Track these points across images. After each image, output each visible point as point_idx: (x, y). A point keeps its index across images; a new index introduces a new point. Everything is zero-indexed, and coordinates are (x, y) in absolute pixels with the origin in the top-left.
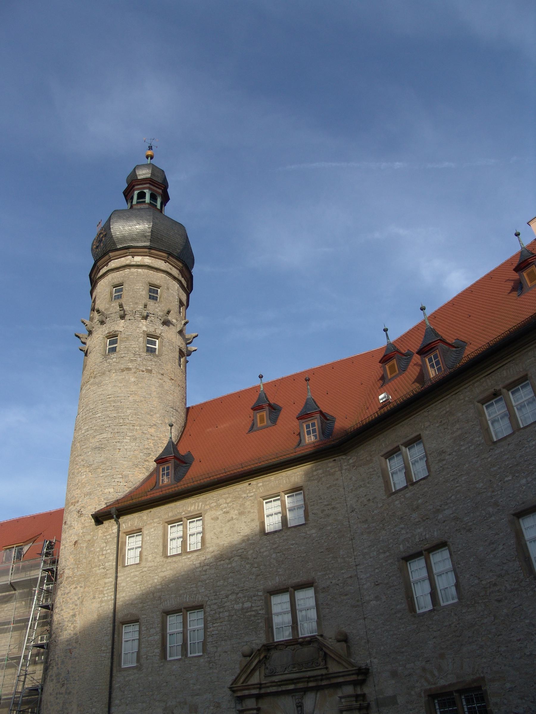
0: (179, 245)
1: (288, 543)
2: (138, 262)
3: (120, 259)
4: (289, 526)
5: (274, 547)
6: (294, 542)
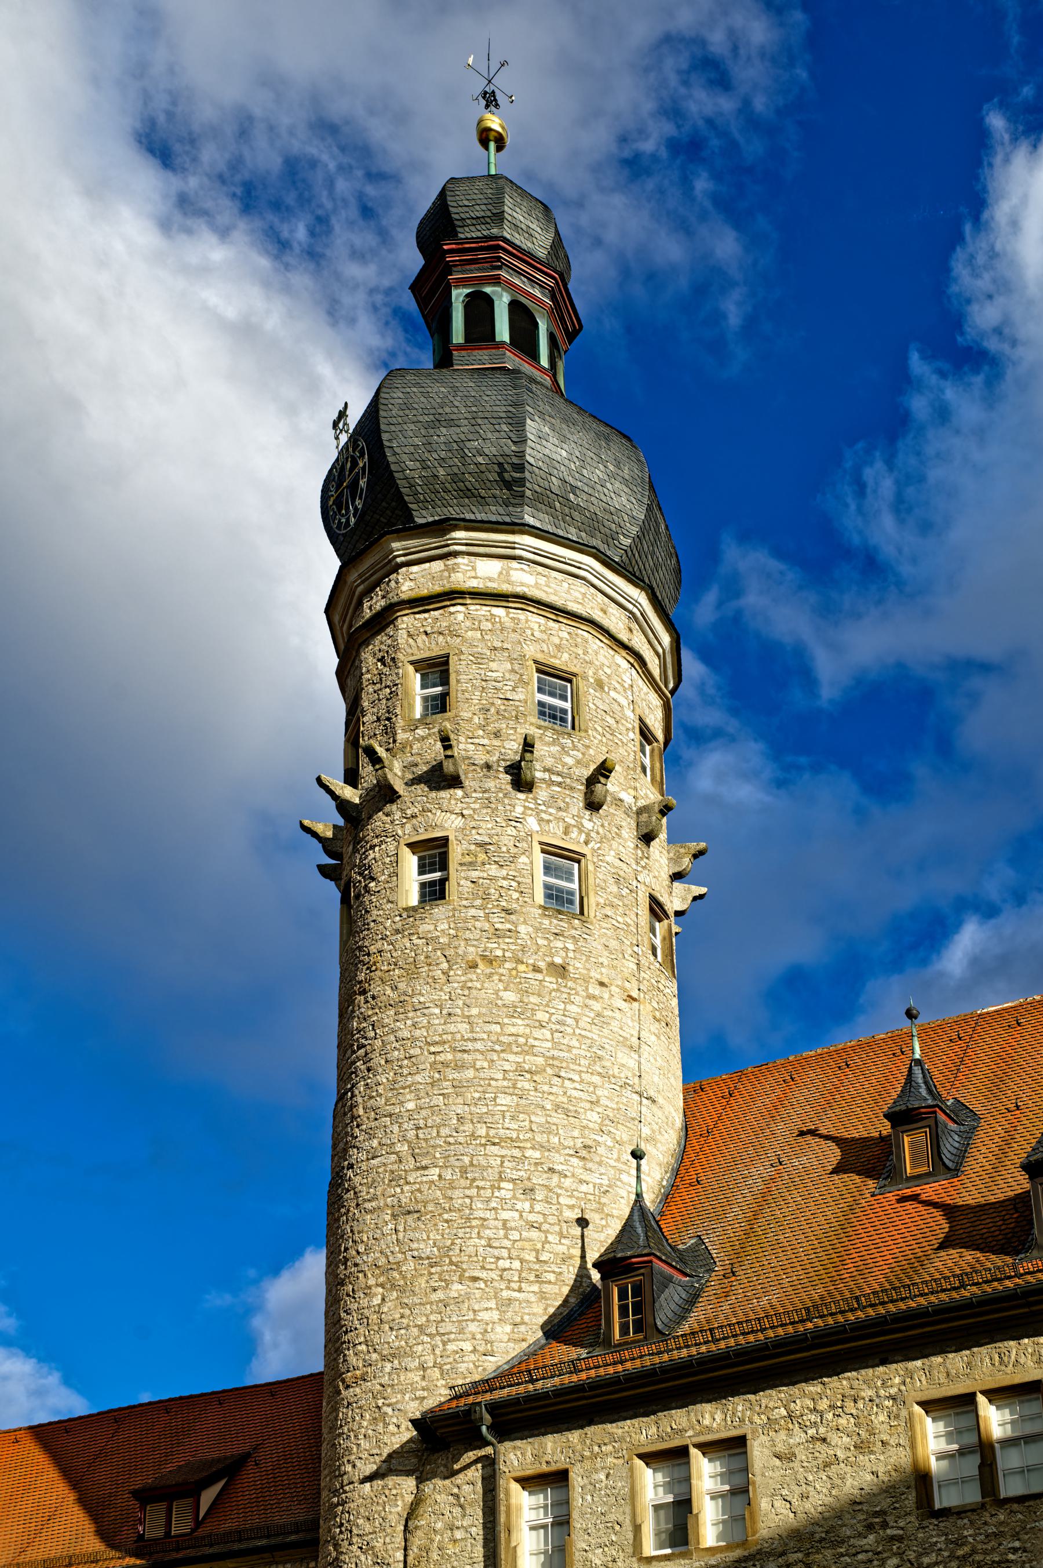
0: (626, 518)
1: (1000, 1544)
2: (490, 579)
3: (427, 565)
4: (1003, 1495)
5: (960, 1553)
6: (1017, 1544)
